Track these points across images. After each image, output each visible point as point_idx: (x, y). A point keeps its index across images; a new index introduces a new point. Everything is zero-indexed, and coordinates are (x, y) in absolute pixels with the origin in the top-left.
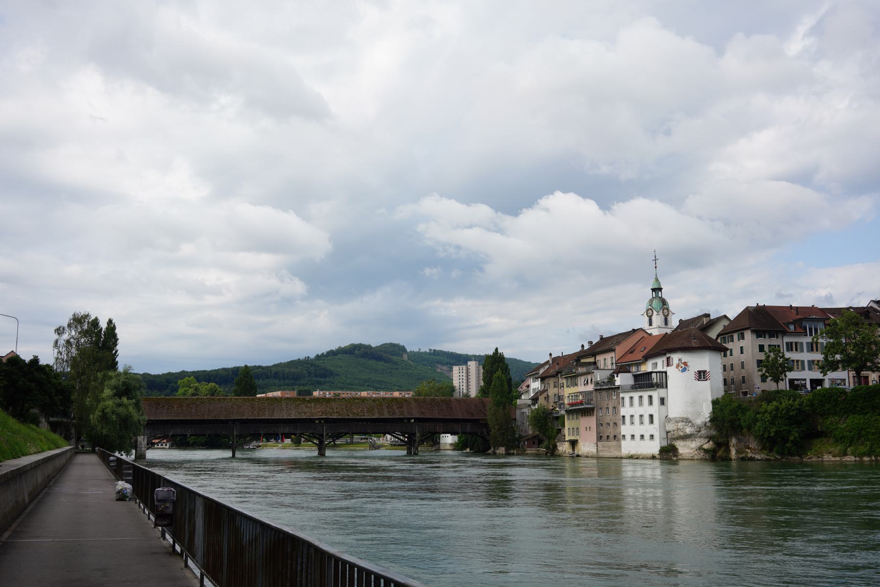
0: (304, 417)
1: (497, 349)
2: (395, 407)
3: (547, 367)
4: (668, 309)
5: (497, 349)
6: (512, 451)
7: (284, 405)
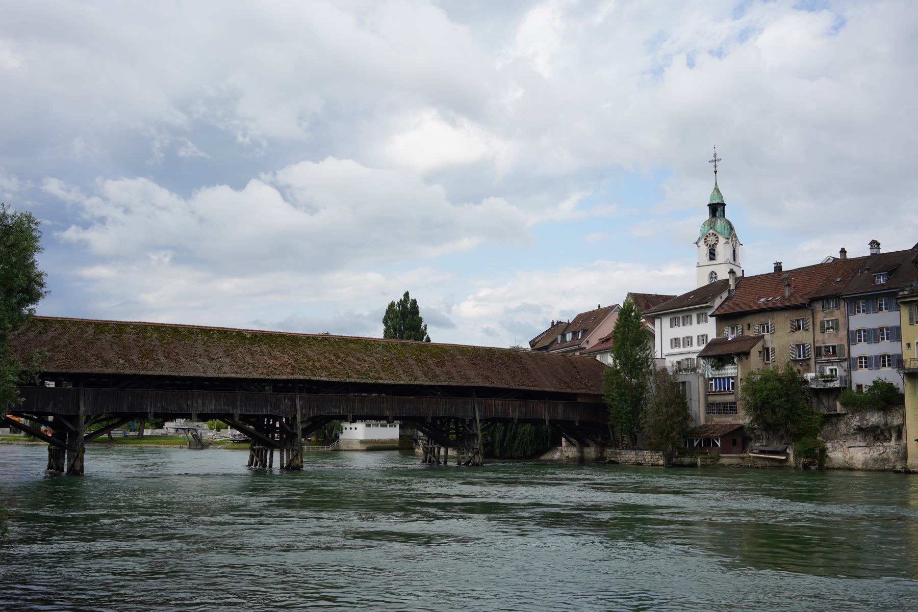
0: (256, 375)
1: (407, 295)
2: (430, 363)
3: (725, 295)
4: (736, 237)
5: (407, 295)
6: (687, 460)
7: (200, 348)
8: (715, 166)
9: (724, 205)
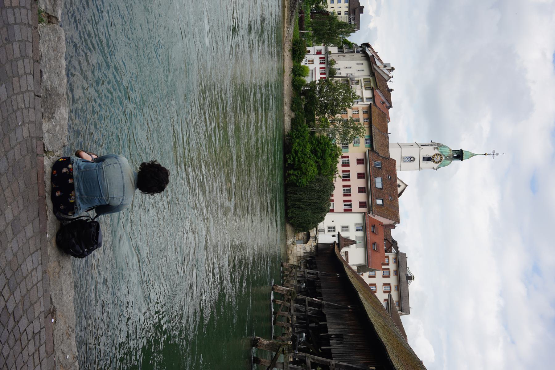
8: (490, 154)
9: (462, 160)
